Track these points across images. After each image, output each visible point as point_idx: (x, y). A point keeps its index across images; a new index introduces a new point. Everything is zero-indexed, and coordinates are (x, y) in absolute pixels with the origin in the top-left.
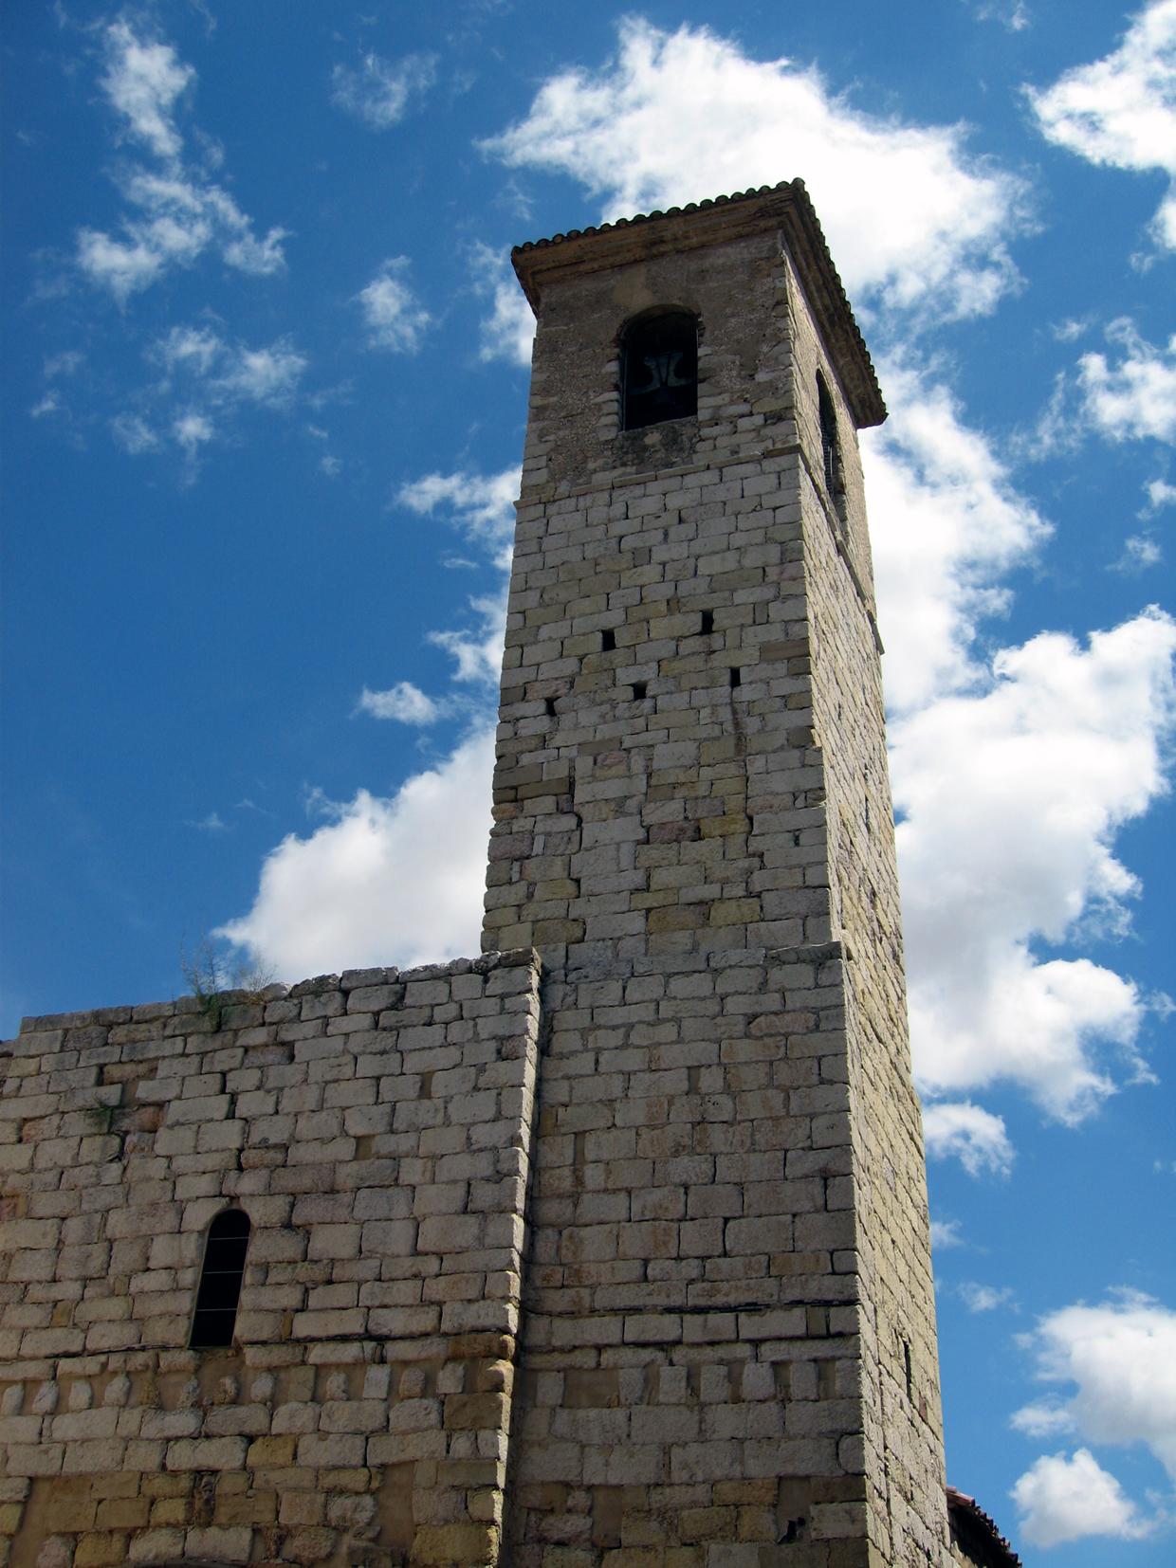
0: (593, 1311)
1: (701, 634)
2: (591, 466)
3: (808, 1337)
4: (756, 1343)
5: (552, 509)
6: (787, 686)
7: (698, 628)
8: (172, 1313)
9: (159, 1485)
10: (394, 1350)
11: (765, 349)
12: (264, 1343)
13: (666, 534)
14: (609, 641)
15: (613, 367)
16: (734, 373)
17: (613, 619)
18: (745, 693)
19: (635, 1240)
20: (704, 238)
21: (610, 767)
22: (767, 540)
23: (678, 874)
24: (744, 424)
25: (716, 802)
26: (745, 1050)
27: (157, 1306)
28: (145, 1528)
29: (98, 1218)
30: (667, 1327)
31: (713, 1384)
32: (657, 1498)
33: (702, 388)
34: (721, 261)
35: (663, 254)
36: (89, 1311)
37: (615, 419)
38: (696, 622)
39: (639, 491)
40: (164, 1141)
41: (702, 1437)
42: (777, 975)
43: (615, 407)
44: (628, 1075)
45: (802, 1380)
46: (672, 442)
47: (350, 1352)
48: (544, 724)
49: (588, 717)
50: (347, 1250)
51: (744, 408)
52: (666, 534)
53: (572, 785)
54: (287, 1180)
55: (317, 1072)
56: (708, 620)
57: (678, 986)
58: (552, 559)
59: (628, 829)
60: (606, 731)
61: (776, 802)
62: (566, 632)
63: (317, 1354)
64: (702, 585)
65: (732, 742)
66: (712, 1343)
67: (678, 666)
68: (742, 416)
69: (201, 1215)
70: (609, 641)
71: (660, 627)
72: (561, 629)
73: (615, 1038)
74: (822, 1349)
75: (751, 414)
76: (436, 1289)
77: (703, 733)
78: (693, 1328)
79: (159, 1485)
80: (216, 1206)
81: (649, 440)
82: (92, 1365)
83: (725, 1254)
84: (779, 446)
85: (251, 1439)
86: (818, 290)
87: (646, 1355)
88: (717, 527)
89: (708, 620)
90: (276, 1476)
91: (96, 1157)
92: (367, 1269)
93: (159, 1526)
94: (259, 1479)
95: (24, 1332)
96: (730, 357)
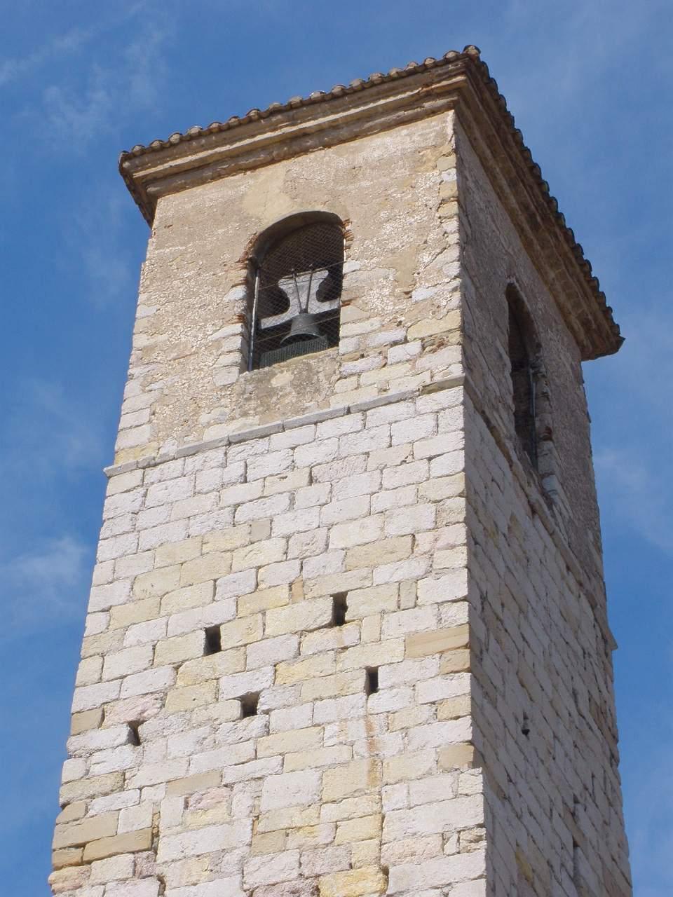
1: (330, 625)
2: (204, 418)
5: (153, 474)
7: (328, 617)
11: (426, 258)
13: (292, 500)
14: (213, 642)
15: (240, 292)
16: (387, 291)
18: (380, 701)
21: (205, 810)
22: (420, 498)
24: (396, 353)
25: (341, 851)
33: (345, 314)
34: (376, 154)
37: (237, 357)
38: (325, 611)
39: (261, 445)
43: (239, 340)
46: (304, 384)
49: (181, 744)
51: (398, 334)
52: (292, 500)
53: (155, 835)
58: (148, 539)
60: (202, 762)
61: (419, 846)
62: (158, 632)
64: (333, 561)
65: (365, 766)
67: (299, 669)
68: (395, 343)
70: (213, 642)
71: (279, 621)
72: (154, 630)
75: (406, 341)
77: (328, 756)
81: (275, 382)
84: (438, 378)
86: (512, 184)
88: (358, 485)
96: (382, 272)
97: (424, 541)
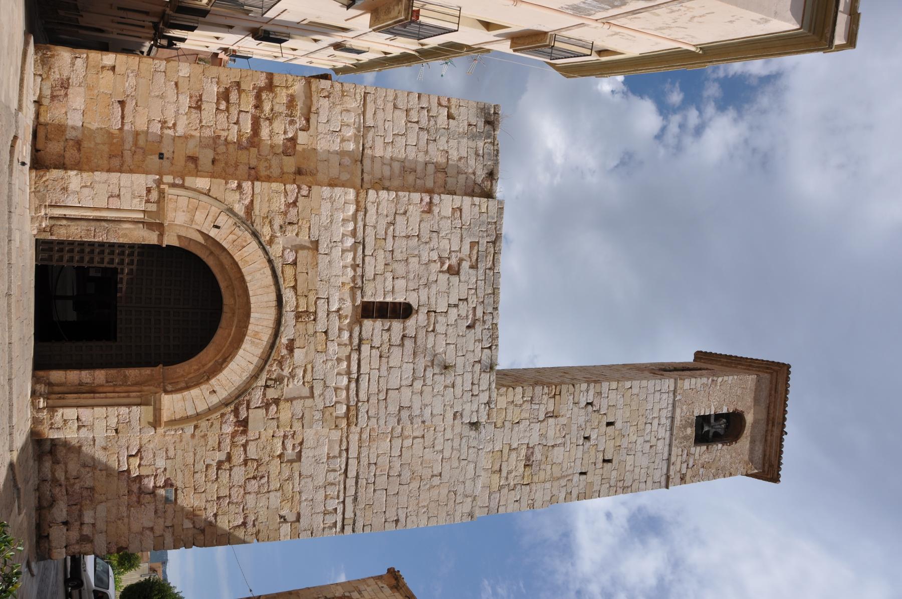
0: (360, 447)
3: (344, 519)
4: (344, 502)
6: (574, 494)
8: (375, 294)
9: (312, 298)
10: (353, 385)
12: (360, 333)
14: (609, 424)
17: (618, 425)
18: (576, 477)
19: (384, 461)
20: (769, 442)
23: (515, 463)
26: (444, 491)
27: (380, 287)
28: (296, 293)
29: (416, 253)
30: (352, 473)
31: (332, 491)
32: (296, 474)
35: (768, 425)
36: (381, 255)
40: (444, 277)
41: (317, 488)
42: (470, 499)
44: (442, 451)
45: (330, 520)
47: (354, 368)
48: (583, 404)
49: (581, 420)
54: (421, 334)
55: (461, 341)
56: (609, 461)
57: (472, 466)
59: (535, 440)
63: (355, 356)
66: (345, 488)
70: (609, 424)
73: (456, 445)
74: (339, 525)
76: (374, 400)
77: (565, 465)
78: (351, 482)
79: (312, 298)
80: (415, 307)
82: (359, 261)
83: (375, 490)
85: (326, 332)
87: (343, 467)
89: (609, 461)
90: (312, 347)
91: (442, 247)
92: (384, 372)
93: (297, 300)
95: (375, 227)
97: (620, 484)
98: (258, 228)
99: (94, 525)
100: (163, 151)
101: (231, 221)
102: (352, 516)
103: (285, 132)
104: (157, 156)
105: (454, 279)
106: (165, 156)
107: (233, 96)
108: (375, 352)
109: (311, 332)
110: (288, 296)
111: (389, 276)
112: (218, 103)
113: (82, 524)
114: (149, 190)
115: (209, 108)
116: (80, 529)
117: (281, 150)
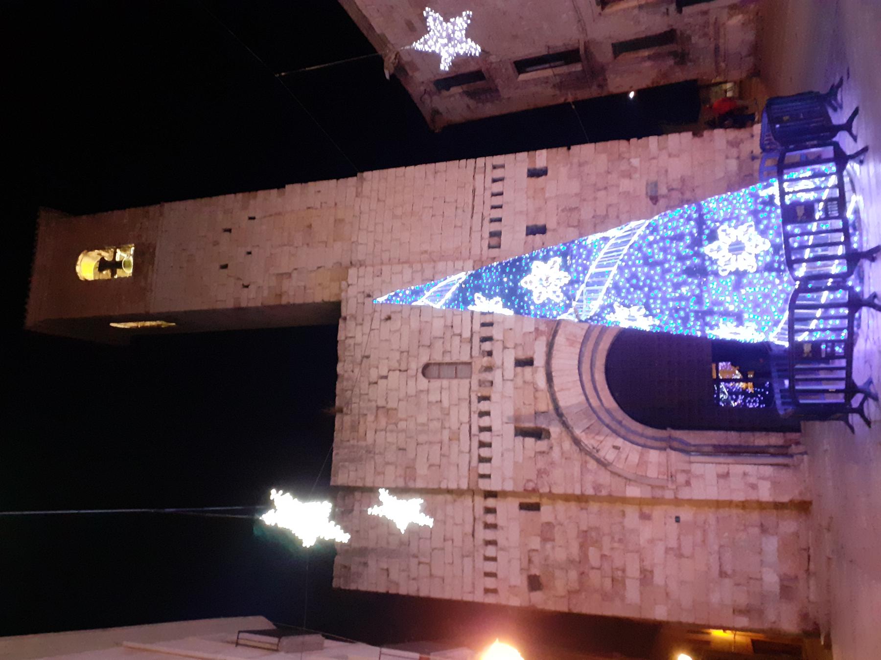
50: (442, 321)
69: (423, 383)
79: (519, 381)
80: (420, 375)
85: (505, 348)
93: (533, 378)
94: (519, 341)
98: (575, 447)
99: (727, 158)
100: (676, 524)
101: (601, 454)
102: (476, 176)
103: (553, 548)
104: (682, 519)
105: (381, 403)
106: (674, 520)
107: (608, 583)
108: (457, 331)
109: (520, 348)
110: (542, 382)
111: (446, 403)
112: (623, 579)
113: (738, 158)
114: (688, 483)
115: (633, 571)
116: (739, 152)
117: (556, 529)
